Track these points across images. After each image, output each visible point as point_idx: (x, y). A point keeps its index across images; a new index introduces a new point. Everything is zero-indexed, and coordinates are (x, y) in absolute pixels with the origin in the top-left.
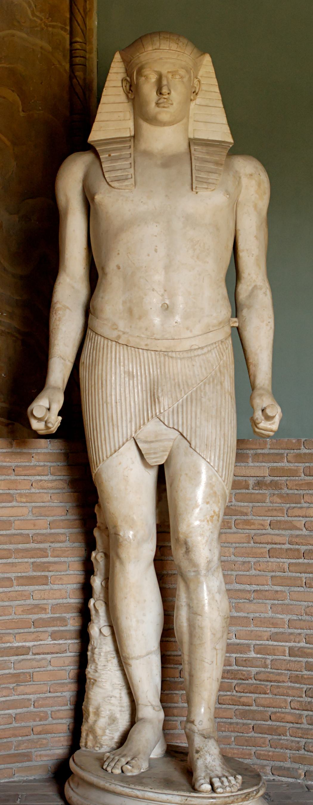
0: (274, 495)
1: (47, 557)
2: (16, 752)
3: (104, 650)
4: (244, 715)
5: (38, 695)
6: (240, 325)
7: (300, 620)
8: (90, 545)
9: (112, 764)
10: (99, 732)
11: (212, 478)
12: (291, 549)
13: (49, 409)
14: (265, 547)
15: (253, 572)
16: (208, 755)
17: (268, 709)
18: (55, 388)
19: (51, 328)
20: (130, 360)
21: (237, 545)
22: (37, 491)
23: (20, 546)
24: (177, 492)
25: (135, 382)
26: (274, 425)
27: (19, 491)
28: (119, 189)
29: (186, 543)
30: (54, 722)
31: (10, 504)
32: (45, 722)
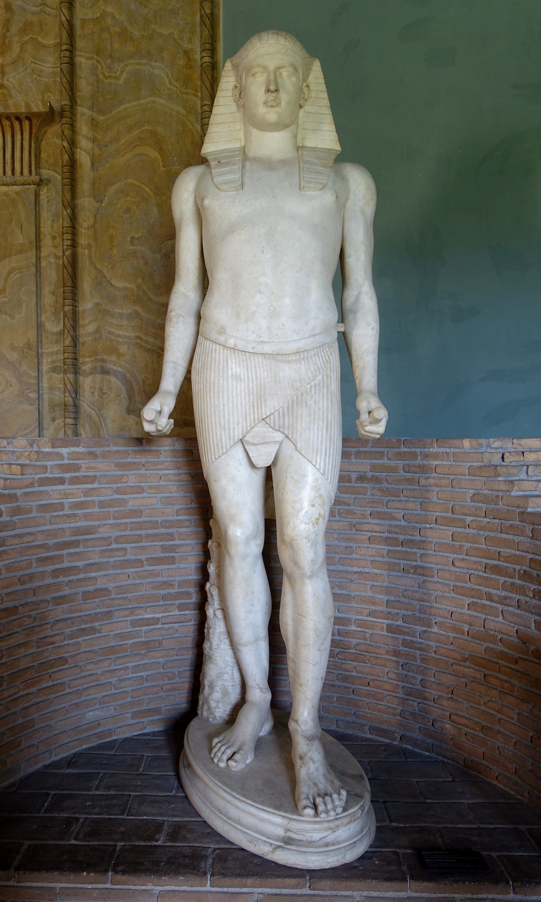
1: (174, 540)
2: (147, 708)
3: (218, 631)
5: (167, 659)
6: (346, 330)
9: (219, 754)
10: (213, 704)
11: (318, 481)
12: (390, 538)
14: (366, 535)
16: (312, 763)
20: (238, 364)
21: (341, 532)
22: (166, 483)
24: (282, 494)
25: (243, 385)
26: (380, 429)
27: (148, 484)
28: (226, 191)
29: (292, 546)
31: (141, 495)
32: (175, 681)
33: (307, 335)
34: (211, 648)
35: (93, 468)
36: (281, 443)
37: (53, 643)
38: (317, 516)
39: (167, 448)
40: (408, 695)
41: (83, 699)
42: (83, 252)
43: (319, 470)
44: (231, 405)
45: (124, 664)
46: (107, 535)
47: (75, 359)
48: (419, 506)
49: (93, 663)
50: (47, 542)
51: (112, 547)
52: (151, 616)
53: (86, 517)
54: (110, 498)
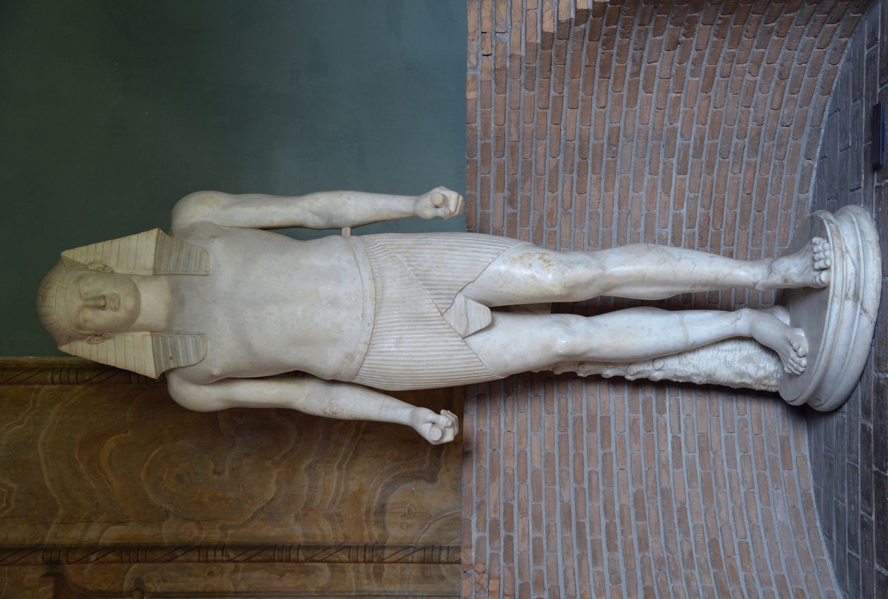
0: (522, 188)
3: (678, 367)
4: (745, 220)
5: (722, 428)
7: (650, 163)
8: (571, 377)
9: (795, 365)
10: (761, 373)
12: (578, 172)
13: (434, 423)
15: (600, 210)
17: (740, 196)
18: (413, 415)
19: (350, 418)
23: (571, 444)
30: (749, 412)
31: (529, 454)
32: (749, 420)
33: (356, 269)
34: (699, 375)
35: (495, 506)
36: (467, 297)
37: (691, 553)
38: (541, 261)
39: (475, 424)
40: (757, 153)
41: (761, 524)
42: (232, 535)
43: (494, 259)
44: (428, 349)
45: (724, 477)
46: (572, 493)
47: (365, 547)
48: (542, 141)
49: (720, 510)
50: (575, 556)
51: (587, 487)
52: (670, 445)
53: (551, 514)
54: (530, 488)
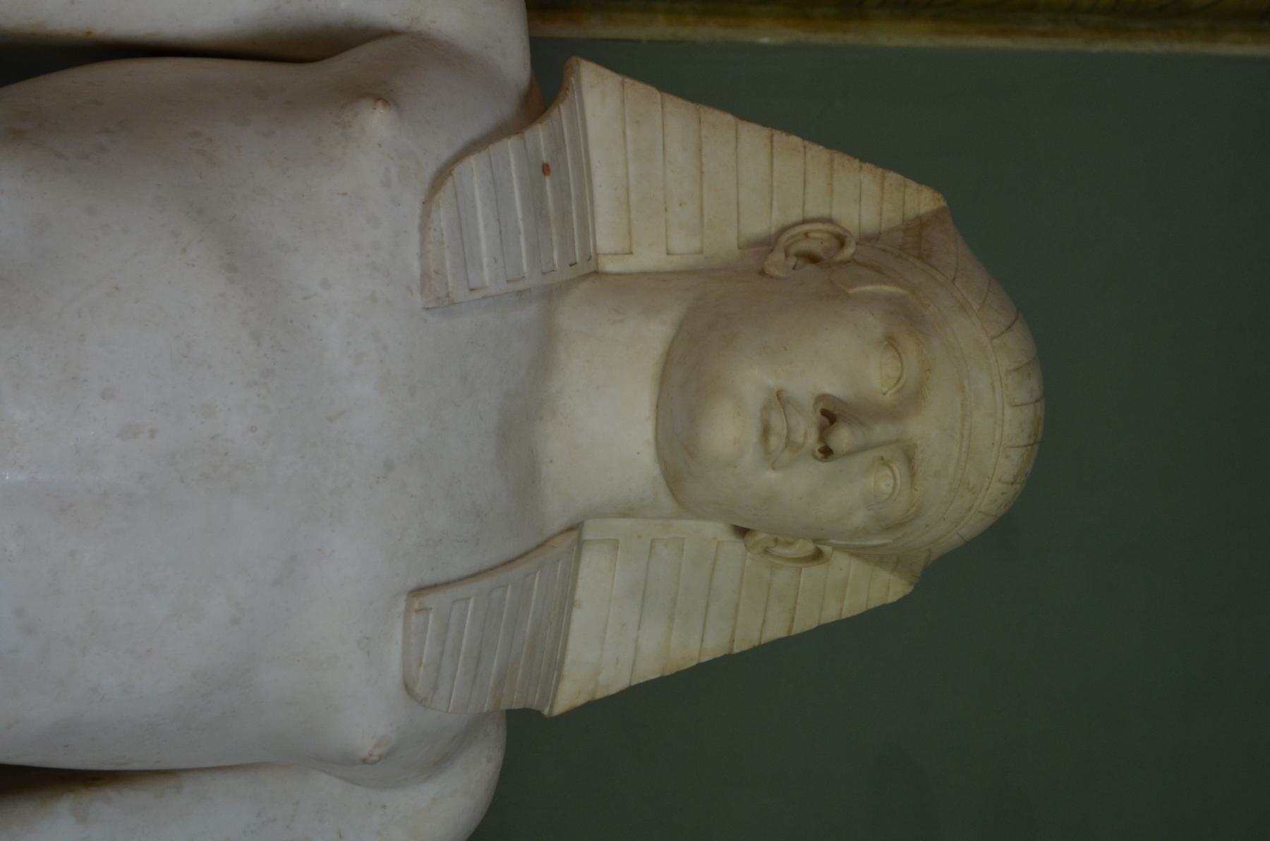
28: (424, 228)
